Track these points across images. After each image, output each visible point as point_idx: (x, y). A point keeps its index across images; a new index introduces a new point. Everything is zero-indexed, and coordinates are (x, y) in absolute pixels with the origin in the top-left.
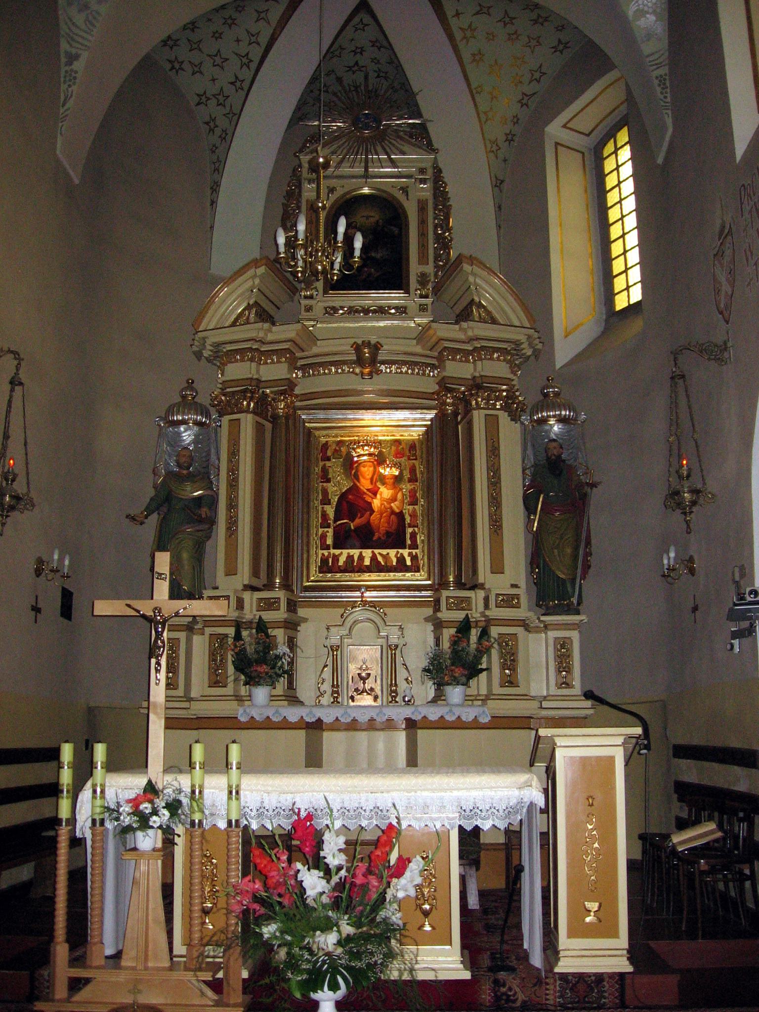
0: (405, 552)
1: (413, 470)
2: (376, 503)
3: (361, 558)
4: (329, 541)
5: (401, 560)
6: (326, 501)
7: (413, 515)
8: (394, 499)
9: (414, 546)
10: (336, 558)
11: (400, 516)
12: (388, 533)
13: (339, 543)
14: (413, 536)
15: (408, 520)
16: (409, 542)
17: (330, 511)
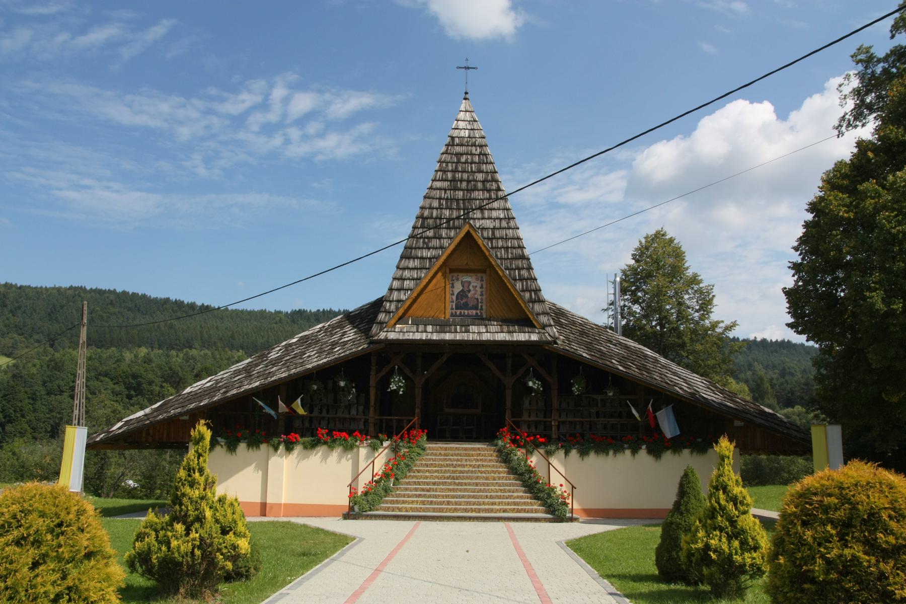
0: (478, 312)
1: (482, 285)
2: (469, 295)
3: (464, 313)
4: (454, 307)
5: (477, 314)
6: (453, 294)
7: (482, 299)
8: (475, 294)
9: (482, 309)
10: (456, 313)
11: (477, 299)
12: (473, 305)
13: (457, 308)
14: (481, 306)
15: (480, 300)
16: (480, 308)
17: (454, 297)
